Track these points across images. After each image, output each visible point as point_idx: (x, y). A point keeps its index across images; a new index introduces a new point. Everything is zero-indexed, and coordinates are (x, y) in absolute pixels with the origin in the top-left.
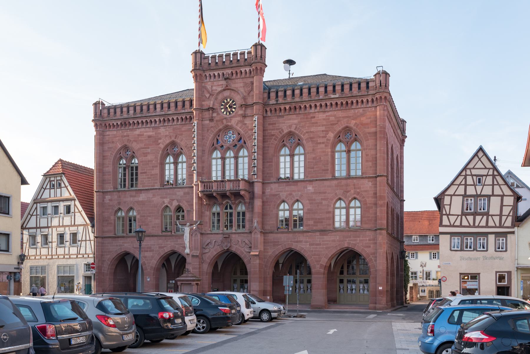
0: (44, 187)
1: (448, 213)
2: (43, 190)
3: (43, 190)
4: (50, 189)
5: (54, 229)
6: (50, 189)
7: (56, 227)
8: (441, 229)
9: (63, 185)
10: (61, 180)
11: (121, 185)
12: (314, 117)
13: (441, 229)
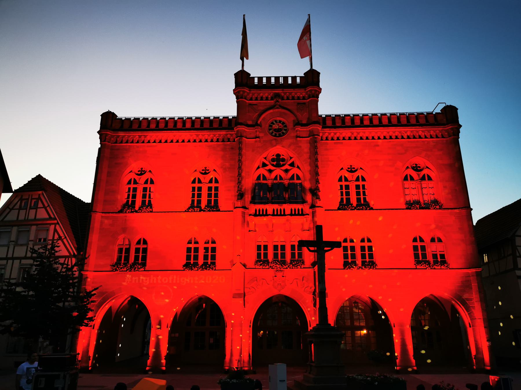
0: (11, 207)
2: (8, 210)
3: (8, 210)
4: (20, 208)
5: (17, 262)
6: (20, 208)
7: (20, 258)
8: (519, 273)
9: (40, 205)
10: (39, 198)
13: (519, 273)
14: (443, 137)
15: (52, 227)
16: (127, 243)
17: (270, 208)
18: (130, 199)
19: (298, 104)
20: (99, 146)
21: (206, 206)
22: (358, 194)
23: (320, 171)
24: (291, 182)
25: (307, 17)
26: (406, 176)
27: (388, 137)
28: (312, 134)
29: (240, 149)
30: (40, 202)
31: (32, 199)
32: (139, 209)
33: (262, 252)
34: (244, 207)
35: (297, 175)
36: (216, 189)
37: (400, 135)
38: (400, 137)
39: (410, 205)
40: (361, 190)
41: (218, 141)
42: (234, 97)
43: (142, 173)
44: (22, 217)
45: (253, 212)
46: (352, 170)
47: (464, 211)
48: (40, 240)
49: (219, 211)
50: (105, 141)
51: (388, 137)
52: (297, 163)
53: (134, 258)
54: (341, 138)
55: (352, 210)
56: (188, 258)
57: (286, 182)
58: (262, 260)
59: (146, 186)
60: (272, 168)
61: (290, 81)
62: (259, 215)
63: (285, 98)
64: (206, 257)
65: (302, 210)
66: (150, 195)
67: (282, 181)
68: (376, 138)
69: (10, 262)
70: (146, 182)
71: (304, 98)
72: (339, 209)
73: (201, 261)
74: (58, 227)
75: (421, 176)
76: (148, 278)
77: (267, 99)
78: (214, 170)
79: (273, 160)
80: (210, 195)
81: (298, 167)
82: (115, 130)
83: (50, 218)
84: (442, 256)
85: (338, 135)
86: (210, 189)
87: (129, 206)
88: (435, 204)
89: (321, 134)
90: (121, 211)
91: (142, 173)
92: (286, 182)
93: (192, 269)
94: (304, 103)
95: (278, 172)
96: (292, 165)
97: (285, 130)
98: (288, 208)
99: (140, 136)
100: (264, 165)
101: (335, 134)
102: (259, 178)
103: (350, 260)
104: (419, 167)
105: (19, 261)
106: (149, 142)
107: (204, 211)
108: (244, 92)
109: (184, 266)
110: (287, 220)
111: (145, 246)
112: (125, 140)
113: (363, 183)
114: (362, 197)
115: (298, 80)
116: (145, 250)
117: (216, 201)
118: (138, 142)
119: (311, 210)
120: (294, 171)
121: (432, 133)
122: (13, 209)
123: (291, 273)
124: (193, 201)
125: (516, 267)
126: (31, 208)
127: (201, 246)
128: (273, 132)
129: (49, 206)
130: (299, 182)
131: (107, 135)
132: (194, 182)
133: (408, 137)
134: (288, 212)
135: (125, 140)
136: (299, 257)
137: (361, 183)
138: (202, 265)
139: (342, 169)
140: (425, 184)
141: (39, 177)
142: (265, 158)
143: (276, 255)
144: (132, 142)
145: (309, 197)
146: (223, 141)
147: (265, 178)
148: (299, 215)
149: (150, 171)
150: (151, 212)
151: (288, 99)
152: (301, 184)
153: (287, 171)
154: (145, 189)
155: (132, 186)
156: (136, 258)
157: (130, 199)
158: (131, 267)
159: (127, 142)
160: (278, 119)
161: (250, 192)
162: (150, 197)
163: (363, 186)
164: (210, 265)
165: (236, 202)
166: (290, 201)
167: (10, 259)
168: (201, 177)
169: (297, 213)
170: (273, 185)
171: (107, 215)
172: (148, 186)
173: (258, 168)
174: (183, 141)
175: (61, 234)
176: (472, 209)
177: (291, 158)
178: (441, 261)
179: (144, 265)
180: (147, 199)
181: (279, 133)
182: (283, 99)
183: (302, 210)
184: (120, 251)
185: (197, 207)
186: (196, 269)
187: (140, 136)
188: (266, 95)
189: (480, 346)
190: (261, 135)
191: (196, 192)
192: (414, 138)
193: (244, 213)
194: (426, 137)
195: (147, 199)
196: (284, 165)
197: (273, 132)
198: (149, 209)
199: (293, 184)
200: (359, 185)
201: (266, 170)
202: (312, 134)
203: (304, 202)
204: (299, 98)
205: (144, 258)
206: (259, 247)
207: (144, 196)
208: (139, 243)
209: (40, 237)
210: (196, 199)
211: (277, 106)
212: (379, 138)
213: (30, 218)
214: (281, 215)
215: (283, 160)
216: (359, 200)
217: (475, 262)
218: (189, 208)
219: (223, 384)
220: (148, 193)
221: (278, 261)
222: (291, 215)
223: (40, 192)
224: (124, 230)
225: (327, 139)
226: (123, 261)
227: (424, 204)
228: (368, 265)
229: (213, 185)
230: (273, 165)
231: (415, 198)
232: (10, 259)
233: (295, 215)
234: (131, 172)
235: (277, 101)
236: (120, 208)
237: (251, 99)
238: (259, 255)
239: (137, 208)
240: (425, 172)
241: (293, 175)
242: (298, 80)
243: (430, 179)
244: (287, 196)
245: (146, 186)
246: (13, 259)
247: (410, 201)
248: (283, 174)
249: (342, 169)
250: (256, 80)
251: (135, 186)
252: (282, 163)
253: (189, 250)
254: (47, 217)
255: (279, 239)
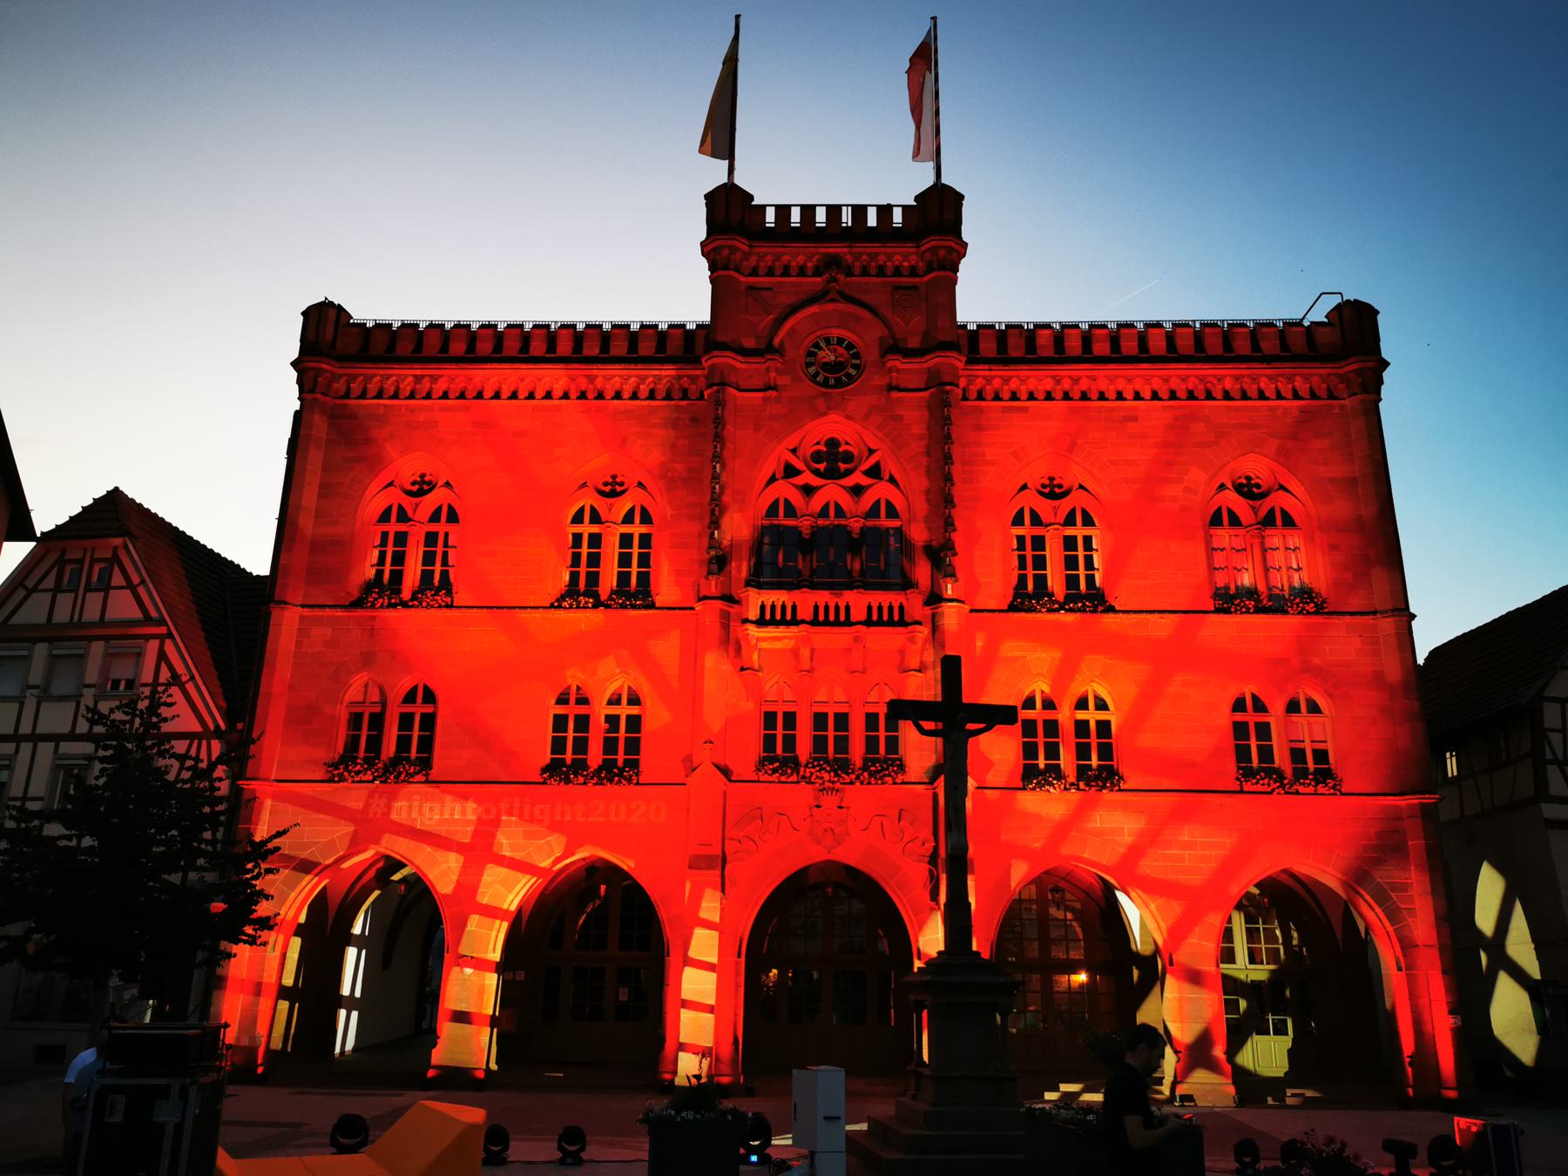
0: (30, 583)
1: (1561, 757)
2: (21, 593)
3: (21, 593)
4: (57, 589)
5: (46, 749)
7: (56, 738)
8: (1550, 811)
9: (118, 579)
10: (115, 559)
11: (446, 544)
12: (1134, 419)
13: (1550, 811)
14: (1331, 396)
15: (153, 645)
16: (375, 696)
17: (807, 601)
18: (388, 568)
19: (897, 288)
20: (297, 405)
21: (613, 592)
22: (1071, 563)
23: (959, 491)
24: (869, 523)
25: (928, 24)
26: (1219, 511)
27: (1164, 394)
28: (937, 383)
29: (719, 421)
30: (116, 569)
31: (93, 561)
32: (414, 597)
33: (780, 732)
34: (729, 598)
35: (837, 504)
36: (645, 540)
37: (1130, 387)
38: (1200, 393)
39: (1228, 601)
40: (1081, 553)
41: (652, 395)
42: (704, 263)
43: (422, 488)
44: (62, 615)
45: (753, 614)
46: (1053, 492)
47: (1387, 625)
48: (116, 684)
49: (652, 606)
50: (313, 391)
51: (1164, 394)
52: (890, 467)
53: (395, 743)
54: (1024, 396)
55: (1049, 611)
56: (558, 745)
57: (855, 525)
58: (778, 758)
59: (433, 527)
60: (816, 481)
61: (872, 221)
62: (773, 622)
63: (857, 271)
64: (610, 745)
65: (901, 607)
66: (445, 555)
67: (843, 522)
68: (1128, 394)
69: (26, 748)
70: (435, 517)
71: (913, 272)
72: (1013, 608)
73: (595, 755)
74: (169, 647)
75: (1262, 513)
76: (437, 806)
77: (802, 272)
78: (640, 484)
79: (817, 457)
80: (625, 560)
81: (892, 480)
82: (344, 359)
83: (148, 619)
84: (1321, 756)
85: (1013, 385)
86: (626, 540)
87: (385, 588)
88: (1306, 600)
89: (963, 382)
90: (358, 604)
91: (422, 488)
92: (855, 525)
93: (568, 781)
94: (915, 287)
95: (832, 492)
96: (874, 472)
97: (855, 367)
98: (858, 601)
99: (418, 379)
100: (790, 472)
101: (1006, 381)
102: (772, 510)
103: (1042, 763)
104: (1258, 486)
105: (51, 745)
106: (445, 396)
107: (608, 606)
108: (734, 249)
109: (544, 770)
110: (856, 639)
111: (429, 709)
112: (373, 388)
113: (1088, 531)
114: (1082, 572)
115: (897, 216)
116: (429, 722)
117: (644, 578)
118: (412, 396)
119: (928, 611)
120: (880, 491)
121: (1299, 383)
122: (35, 589)
123: (863, 798)
124: (574, 577)
125: (1541, 792)
126: (88, 589)
127: (601, 711)
128: (817, 374)
129: (143, 582)
130: (895, 523)
131: (319, 371)
132: (578, 518)
133: (1227, 396)
134: (858, 614)
135: (373, 388)
136: (836, 752)
137: (1079, 532)
138: (600, 769)
139: (1025, 487)
140: (1275, 539)
141: (115, 496)
142: (794, 451)
143: (819, 744)
144: (395, 396)
145: (922, 572)
146: (668, 397)
147: (790, 511)
148: (891, 623)
149: (448, 484)
150: (450, 606)
151: (865, 272)
152: (899, 531)
153: (857, 491)
154: (431, 539)
155: (393, 527)
156: (404, 743)
157: (388, 568)
158: (386, 770)
159: (379, 396)
160: (835, 333)
161: (745, 551)
162: (445, 562)
163: (1088, 541)
164: (622, 771)
165: (703, 582)
166: (864, 583)
167: (26, 738)
168: (600, 504)
169: (778, 617)
170: (816, 531)
171: (317, 612)
172: (441, 528)
173: (773, 479)
174: (548, 396)
175: (180, 668)
176: (1413, 616)
177: (871, 452)
178: (1315, 770)
179: (425, 763)
180: (438, 568)
181: (836, 377)
182: (849, 272)
183: (901, 607)
184: (355, 720)
185: (585, 594)
186: (581, 780)
187: (418, 379)
188: (801, 259)
189: (1428, 1028)
190: (782, 381)
191: (585, 550)
192: (1245, 396)
193: (725, 618)
194: (1279, 397)
195: (438, 568)
196: (849, 472)
197: (817, 374)
198: (442, 598)
199: (876, 529)
200: (1075, 538)
201: (796, 486)
202: (937, 383)
203: (907, 584)
204: (897, 272)
205: (426, 744)
206: (770, 719)
207: (429, 559)
208: (410, 697)
209: (114, 675)
210: (583, 570)
211: (832, 295)
212: (1137, 397)
213: (85, 618)
214: (837, 623)
215: (848, 457)
216: (1072, 582)
217: (1418, 773)
218: (562, 598)
219: (657, 1128)
220: (440, 549)
221: (826, 761)
222: (868, 622)
223: (118, 541)
224: (367, 660)
225: (980, 397)
226: (362, 753)
227: (1270, 597)
228: (1097, 778)
229: (637, 529)
230: (816, 473)
231: (1246, 580)
232: (26, 738)
233: (880, 623)
234: (391, 484)
235: (834, 280)
236: (356, 595)
237: (754, 273)
238: (769, 742)
239: (406, 594)
240: (1278, 500)
241: (877, 504)
242: (897, 216)
243: (1288, 521)
244: (857, 566)
245: (433, 527)
246: (35, 738)
247: (1227, 588)
248: (845, 501)
249: (1025, 487)
250: (770, 216)
251: (402, 527)
252: (842, 466)
253: (560, 722)
254: (139, 615)
255: (831, 695)
